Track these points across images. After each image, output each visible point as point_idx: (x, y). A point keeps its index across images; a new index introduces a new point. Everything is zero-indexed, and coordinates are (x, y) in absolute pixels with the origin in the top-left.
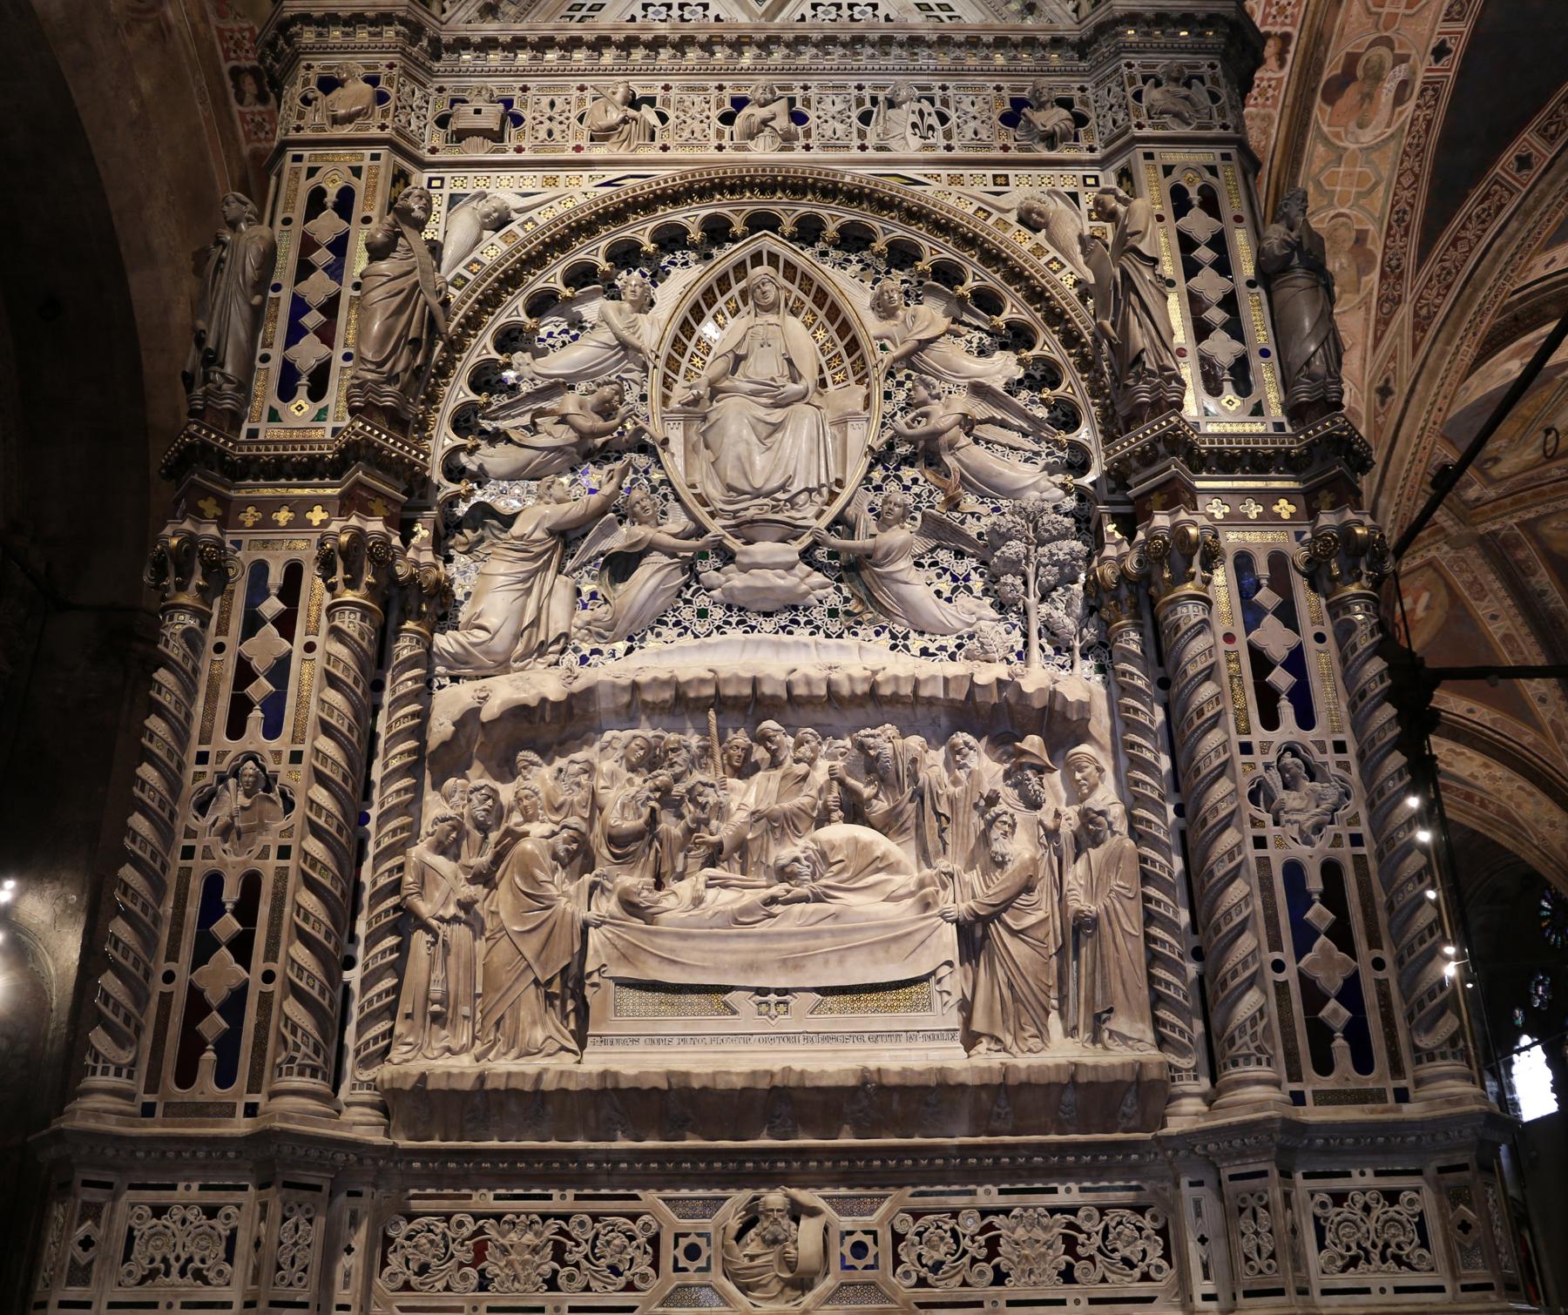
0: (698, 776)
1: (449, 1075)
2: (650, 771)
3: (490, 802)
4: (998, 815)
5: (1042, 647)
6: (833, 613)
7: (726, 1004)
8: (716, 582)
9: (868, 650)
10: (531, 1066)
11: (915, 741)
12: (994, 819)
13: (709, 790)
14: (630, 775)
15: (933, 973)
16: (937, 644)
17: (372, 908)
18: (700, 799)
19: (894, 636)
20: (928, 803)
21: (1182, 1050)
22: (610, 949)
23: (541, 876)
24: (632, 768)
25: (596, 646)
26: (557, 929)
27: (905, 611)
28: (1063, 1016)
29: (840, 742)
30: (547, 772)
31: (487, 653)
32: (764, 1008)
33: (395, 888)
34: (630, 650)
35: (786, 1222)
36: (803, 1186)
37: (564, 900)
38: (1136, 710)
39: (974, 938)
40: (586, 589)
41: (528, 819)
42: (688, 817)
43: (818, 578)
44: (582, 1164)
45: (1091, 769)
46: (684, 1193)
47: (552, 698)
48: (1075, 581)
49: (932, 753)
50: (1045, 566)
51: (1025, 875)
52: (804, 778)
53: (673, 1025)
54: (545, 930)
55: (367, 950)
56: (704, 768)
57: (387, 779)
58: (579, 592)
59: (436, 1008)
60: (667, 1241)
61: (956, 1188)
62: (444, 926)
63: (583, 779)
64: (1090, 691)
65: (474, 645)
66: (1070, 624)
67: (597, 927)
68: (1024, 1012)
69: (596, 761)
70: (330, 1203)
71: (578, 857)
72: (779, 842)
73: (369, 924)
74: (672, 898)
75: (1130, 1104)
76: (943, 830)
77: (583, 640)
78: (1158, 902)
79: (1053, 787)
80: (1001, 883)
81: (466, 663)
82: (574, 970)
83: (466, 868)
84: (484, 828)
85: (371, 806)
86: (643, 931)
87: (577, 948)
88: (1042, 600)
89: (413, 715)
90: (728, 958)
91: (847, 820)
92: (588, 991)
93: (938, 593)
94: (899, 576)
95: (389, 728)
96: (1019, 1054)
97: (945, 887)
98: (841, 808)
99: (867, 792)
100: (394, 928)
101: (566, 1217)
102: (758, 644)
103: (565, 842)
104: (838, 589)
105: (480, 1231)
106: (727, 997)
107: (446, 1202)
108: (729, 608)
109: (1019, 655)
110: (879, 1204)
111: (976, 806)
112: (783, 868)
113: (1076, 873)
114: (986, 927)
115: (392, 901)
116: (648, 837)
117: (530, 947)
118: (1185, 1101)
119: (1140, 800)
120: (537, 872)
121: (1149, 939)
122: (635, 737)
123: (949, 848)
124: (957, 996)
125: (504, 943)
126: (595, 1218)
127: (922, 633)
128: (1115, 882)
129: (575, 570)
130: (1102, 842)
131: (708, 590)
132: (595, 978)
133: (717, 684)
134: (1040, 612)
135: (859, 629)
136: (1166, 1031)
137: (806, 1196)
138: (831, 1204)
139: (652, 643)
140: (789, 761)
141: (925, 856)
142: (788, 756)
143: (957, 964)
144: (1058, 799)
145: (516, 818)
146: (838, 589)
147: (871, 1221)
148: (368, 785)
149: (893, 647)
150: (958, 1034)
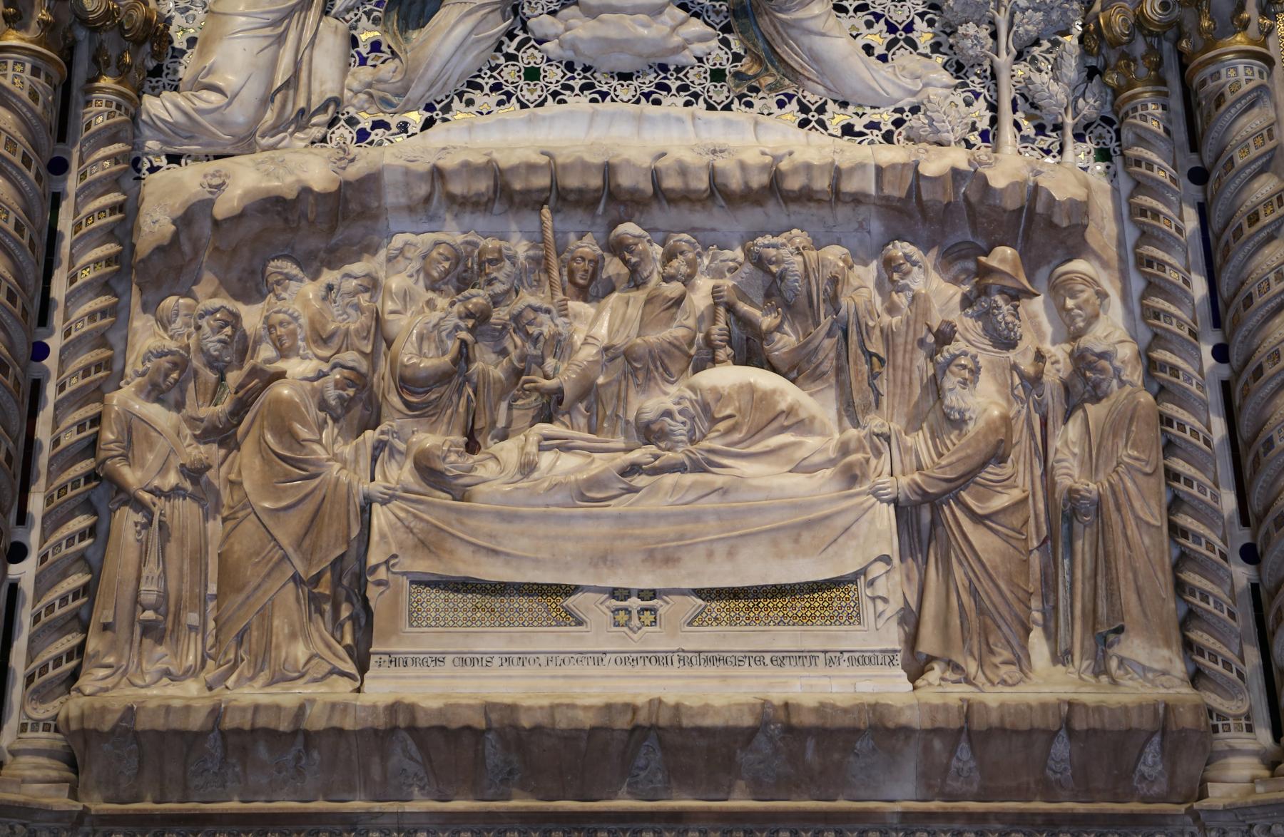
0: (527, 298)
1: (168, 709)
2: (459, 291)
3: (228, 330)
4: (955, 357)
5: (1017, 125)
6: (717, 75)
7: (568, 612)
8: (551, 31)
10: (288, 696)
11: (834, 254)
12: (949, 363)
13: (543, 317)
14: (431, 295)
15: (863, 572)
16: (866, 120)
18: (531, 329)
19: (804, 108)
20: (853, 337)
21: (1227, 690)
22: (402, 534)
23: (304, 433)
25: (381, 116)
26: (327, 505)
27: (821, 73)
28: (1051, 635)
29: (728, 254)
30: (311, 289)
31: (221, 124)
33: (91, 448)
34: (428, 124)
37: (337, 466)
38: (1156, 214)
39: (923, 522)
40: (367, 36)
41: (283, 353)
42: (514, 354)
43: (696, 26)
45: (1088, 293)
47: (317, 187)
48: (1066, 33)
49: (858, 269)
50: (1024, 10)
51: (993, 439)
52: (678, 302)
53: (492, 640)
54: (309, 507)
58: (354, 42)
59: (149, 615)
62: (161, 502)
63: (364, 299)
64: (1087, 186)
66: (1059, 92)
67: (384, 503)
68: (988, 630)
69: (382, 274)
72: (644, 388)
73: (49, 499)
74: (492, 465)
78: (1189, 482)
80: (958, 450)
82: (352, 565)
83: (192, 421)
85: (51, 334)
87: (355, 531)
88: (1019, 57)
89: (114, 208)
90: (570, 547)
91: (737, 361)
92: (372, 592)
93: (868, 49)
94: (812, 25)
95: (78, 226)
96: (988, 687)
97: (878, 454)
98: (729, 343)
100: (88, 506)
103: (337, 385)
104: (725, 42)
106: (571, 601)
108: (570, 66)
109: (984, 136)
111: (922, 343)
113: (1068, 438)
116: (457, 380)
117: (286, 533)
118: (1233, 761)
120: (298, 427)
122: (437, 244)
123: (884, 400)
124: (895, 605)
125: (250, 525)
127: (844, 104)
128: (1127, 453)
129: (348, 10)
130: (1106, 395)
131: (541, 42)
132: (382, 574)
133: (554, 169)
134: (1012, 74)
135: (754, 98)
139: (460, 113)
140: (655, 278)
141: (849, 411)
142: (654, 271)
143: (896, 560)
146: (725, 42)
148: (46, 304)
149: (803, 124)
150: (899, 657)
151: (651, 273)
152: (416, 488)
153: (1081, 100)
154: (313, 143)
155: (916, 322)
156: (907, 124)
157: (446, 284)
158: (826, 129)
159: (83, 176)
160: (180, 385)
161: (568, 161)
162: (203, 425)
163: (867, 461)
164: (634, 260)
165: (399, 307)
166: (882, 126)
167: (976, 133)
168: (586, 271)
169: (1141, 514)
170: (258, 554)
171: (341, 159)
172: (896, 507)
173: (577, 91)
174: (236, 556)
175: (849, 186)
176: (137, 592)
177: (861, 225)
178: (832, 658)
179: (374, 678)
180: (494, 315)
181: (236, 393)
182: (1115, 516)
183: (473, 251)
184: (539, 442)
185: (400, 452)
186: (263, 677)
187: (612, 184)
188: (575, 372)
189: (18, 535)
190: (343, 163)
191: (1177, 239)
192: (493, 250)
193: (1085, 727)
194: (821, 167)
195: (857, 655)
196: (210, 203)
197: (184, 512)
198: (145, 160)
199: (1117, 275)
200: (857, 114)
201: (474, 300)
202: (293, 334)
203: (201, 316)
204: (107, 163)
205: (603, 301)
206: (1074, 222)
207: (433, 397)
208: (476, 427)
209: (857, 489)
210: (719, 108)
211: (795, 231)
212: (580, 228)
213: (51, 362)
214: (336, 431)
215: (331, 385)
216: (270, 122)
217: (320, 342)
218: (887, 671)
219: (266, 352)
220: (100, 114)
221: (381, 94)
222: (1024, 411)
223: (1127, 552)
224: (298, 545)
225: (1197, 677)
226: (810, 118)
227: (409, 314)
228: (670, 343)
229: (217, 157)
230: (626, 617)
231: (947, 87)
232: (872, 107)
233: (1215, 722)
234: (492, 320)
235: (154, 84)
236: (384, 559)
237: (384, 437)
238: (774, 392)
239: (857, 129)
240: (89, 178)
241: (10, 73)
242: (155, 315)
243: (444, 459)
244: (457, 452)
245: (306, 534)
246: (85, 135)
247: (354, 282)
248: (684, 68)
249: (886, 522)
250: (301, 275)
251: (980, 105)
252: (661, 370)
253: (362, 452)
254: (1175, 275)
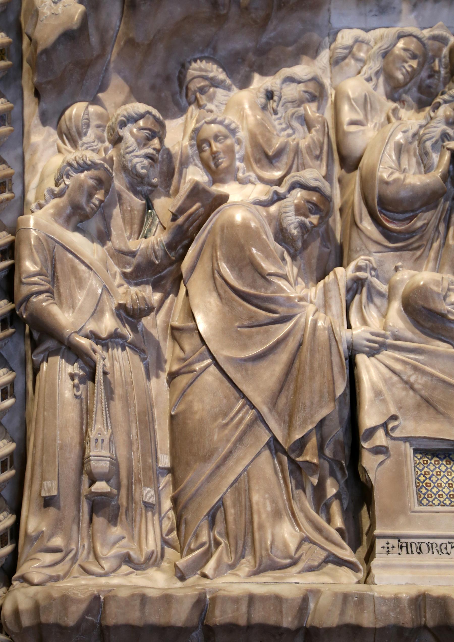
1: (143, 599)
14: (392, 105)
22: (400, 391)
23: (268, 267)
54: (283, 357)
59: (101, 486)
63: (311, 109)
67: (372, 353)
71: (319, 245)
83: (122, 255)
87: (341, 387)
92: (368, 461)
103: (299, 210)
117: (261, 384)
132: (380, 438)
152: (409, 334)
157: (406, 92)
160: (104, 211)
162: (134, 261)
165: (360, 116)
170: (225, 415)
174: (197, 417)
176: (83, 460)
179: (384, 566)
181: (175, 218)
183: (440, 49)
185: (381, 294)
186: (246, 566)
197: (120, 363)
202: (230, 151)
203: (123, 124)
207: (419, 224)
215: (291, 210)
217: (265, 161)
219: (195, 175)
224: (273, 403)
236: (381, 421)
237: (361, 274)
242: (57, 127)
243: (445, 297)
245: (280, 391)
250: (228, 81)
253: (333, 293)
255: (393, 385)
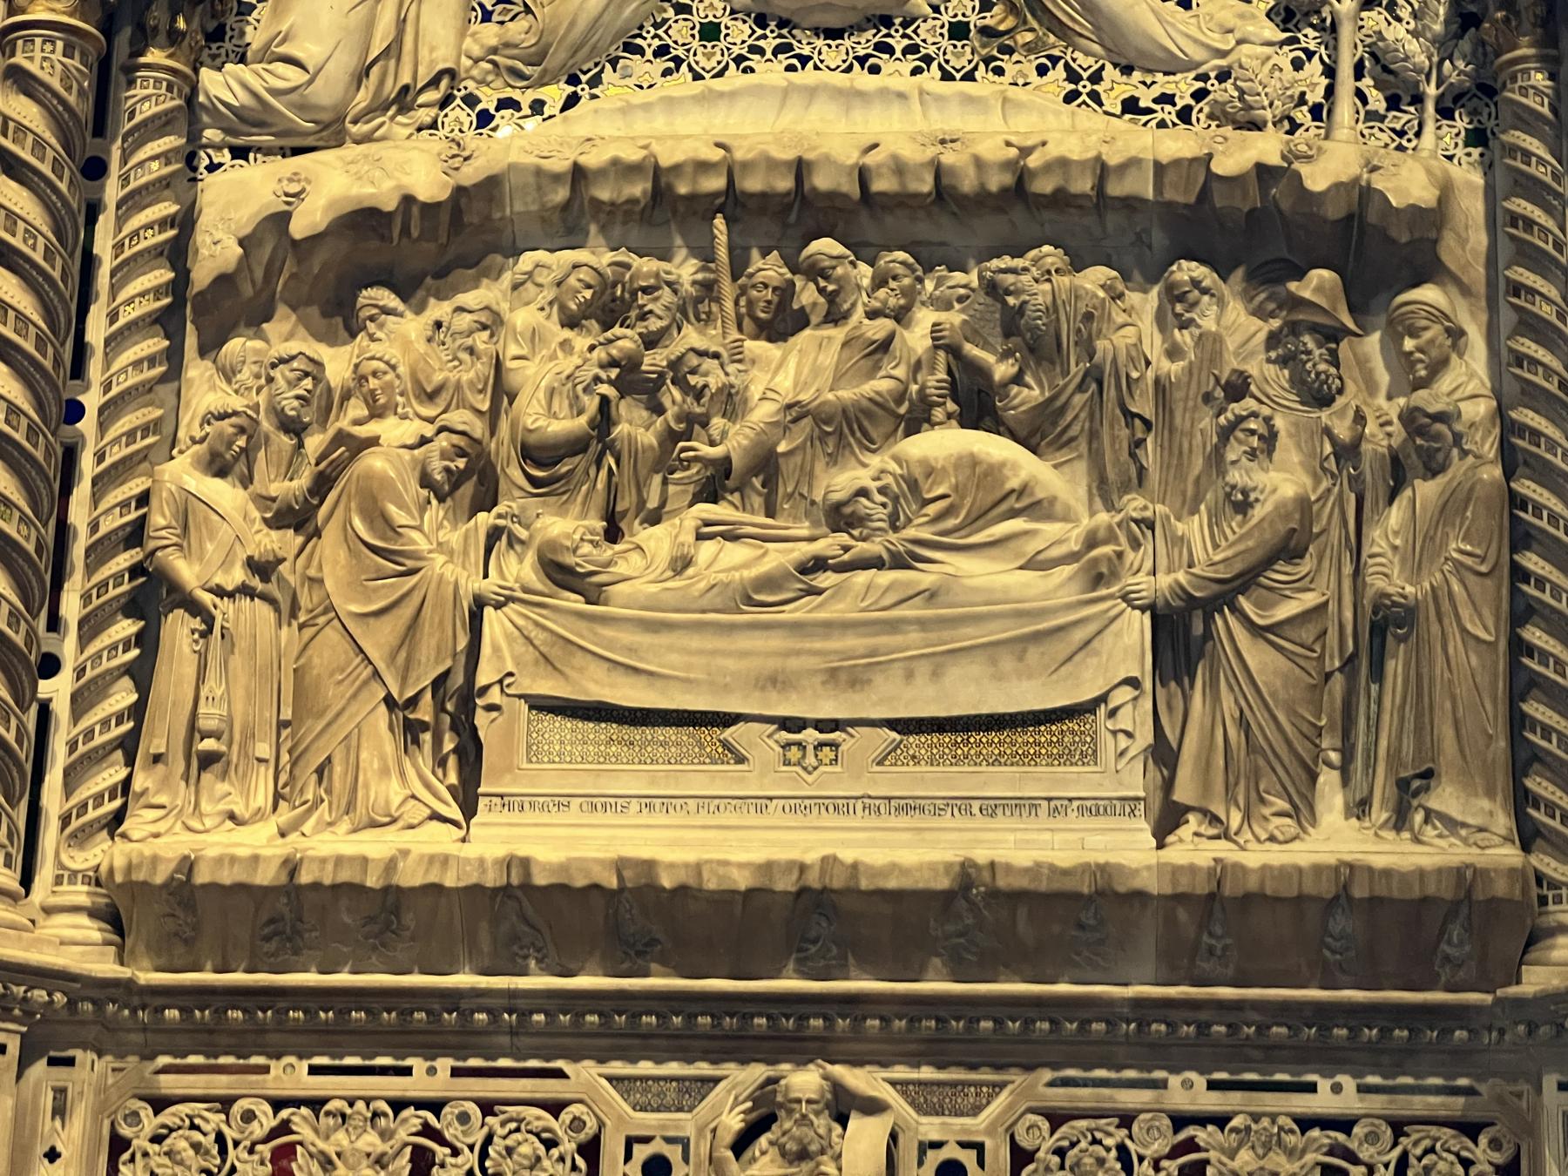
0: (691, 337)
3: (308, 383)
4: (1241, 419)
5: (1361, 95)
6: (958, 31)
7: (725, 745)
9: (1019, 105)
10: (376, 845)
11: (1095, 278)
13: (709, 364)
14: (567, 333)
16: (1156, 91)
17: (90, 570)
18: (693, 380)
19: (1073, 76)
20: (1110, 394)
23: (399, 516)
24: (571, 322)
27: (1097, 28)
29: (958, 277)
31: (302, 108)
32: (794, 753)
33: (135, 534)
34: (571, 101)
35: (822, 1123)
36: (856, 1062)
38: (1529, 224)
41: (376, 413)
42: (671, 412)
44: (467, 1015)
45: (1435, 331)
46: (646, 1067)
49: (1134, 297)
51: (1282, 528)
54: (407, 611)
55: (84, 640)
56: (705, 320)
57: (115, 342)
59: (209, 744)
60: (612, 1148)
61: (1131, 1074)
62: (224, 604)
63: (481, 340)
65: (275, 92)
68: (1277, 774)
69: (504, 307)
70: (19, 1077)
72: (833, 460)
73: (86, 598)
74: (635, 557)
75: (1456, 942)
76: (1140, 443)
77: (482, 82)
78: (1541, 583)
79: (1362, 363)
81: (261, 125)
83: (263, 500)
84: (294, 428)
85: (87, 388)
86: (580, 615)
87: (462, 643)
89: (164, 223)
90: (731, 664)
92: (481, 719)
95: (119, 247)
96: (1253, 845)
99: (1002, 371)
100: (132, 607)
101: (436, 1106)
102: (812, 92)
103: (444, 455)
105: (284, 1128)
106: (728, 733)
107: (223, 1079)
108: (761, 21)
109: (1316, 112)
110: (990, 1098)
111: (1208, 398)
112: (837, 508)
114: (1208, 620)
115: (124, 560)
116: (595, 447)
117: (378, 641)
119: (1532, 396)
120: (392, 509)
121: (1519, 648)
122: (576, 266)
125: (332, 635)
126: (488, 1108)
127: (1127, 70)
132: (495, 696)
135: (1006, 63)
136: (1539, 815)
137: (861, 1080)
138: (904, 1094)
141: (1104, 491)
144: (1371, 387)
145: (357, 409)
147: (976, 1125)
149: (1070, 97)
151: (854, 305)
152: (539, 586)
153: (1447, 63)
154: (419, 130)
155: (1201, 369)
156: (1211, 97)
158: (1101, 104)
159: (125, 180)
161: (750, 156)
162: (275, 506)
163: (1120, 555)
164: (831, 288)
166: (1177, 99)
167: (1305, 108)
168: (769, 302)
169: (1469, 627)
170: (343, 671)
171: (454, 156)
172: (1154, 618)
173: (769, 55)
174: (315, 672)
175: (1115, 189)
177: (1138, 235)
178: (1057, 806)
180: (647, 360)
181: (317, 464)
182: (1435, 628)
183: (623, 275)
184: (698, 528)
185: (522, 542)
186: (345, 825)
187: (806, 187)
188: (746, 437)
189: (48, 642)
190: (457, 162)
191: (1554, 259)
192: (648, 276)
193: (1366, 895)
194: (1082, 164)
195: (1089, 803)
196: (281, 220)
198: (202, 154)
199: (1483, 303)
200: (1144, 83)
201: (620, 343)
203: (274, 366)
204: (155, 165)
205: (792, 340)
206: (1417, 235)
208: (619, 508)
209: (1103, 592)
210: (958, 76)
211: (1047, 248)
212: (766, 242)
213: (87, 425)
214: (441, 514)
215: (437, 453)
216: (363, 105)
217: (424, 397)
218: (1126, 822)
219: (357, 409)
220: (147, 98)
221: (510, 62)
222: (1336, 489)
223: (1447, 675)
224: (392, 658)
225: (1528, 836)
226: (1080, 90)
227: (537, 360)
228: (870, 400)
229: (297, 151)
230: (799, 754)
231: (1269, 44)
232: (1166, 74)
233: (1545, 891)
234: (644, 368)
235: (214, 51)
236: (497, 678)
237: (501, 522)
238: (1003, 465)
239: (1142, 104)
240: (133, 185)
241: (38, 55)
242: (214, 362)
243: (575, 551)
244: (591, 542)
245: (400, 647)
246: (128, 126)
247: (468, 317)
248: (914, 20)
249: (1136, 635)
250: (401, 307)
251: (1314, 68)
252: (858, 434)
253: (472, 541)
254: (1547, 308)
255: (514, 640)
